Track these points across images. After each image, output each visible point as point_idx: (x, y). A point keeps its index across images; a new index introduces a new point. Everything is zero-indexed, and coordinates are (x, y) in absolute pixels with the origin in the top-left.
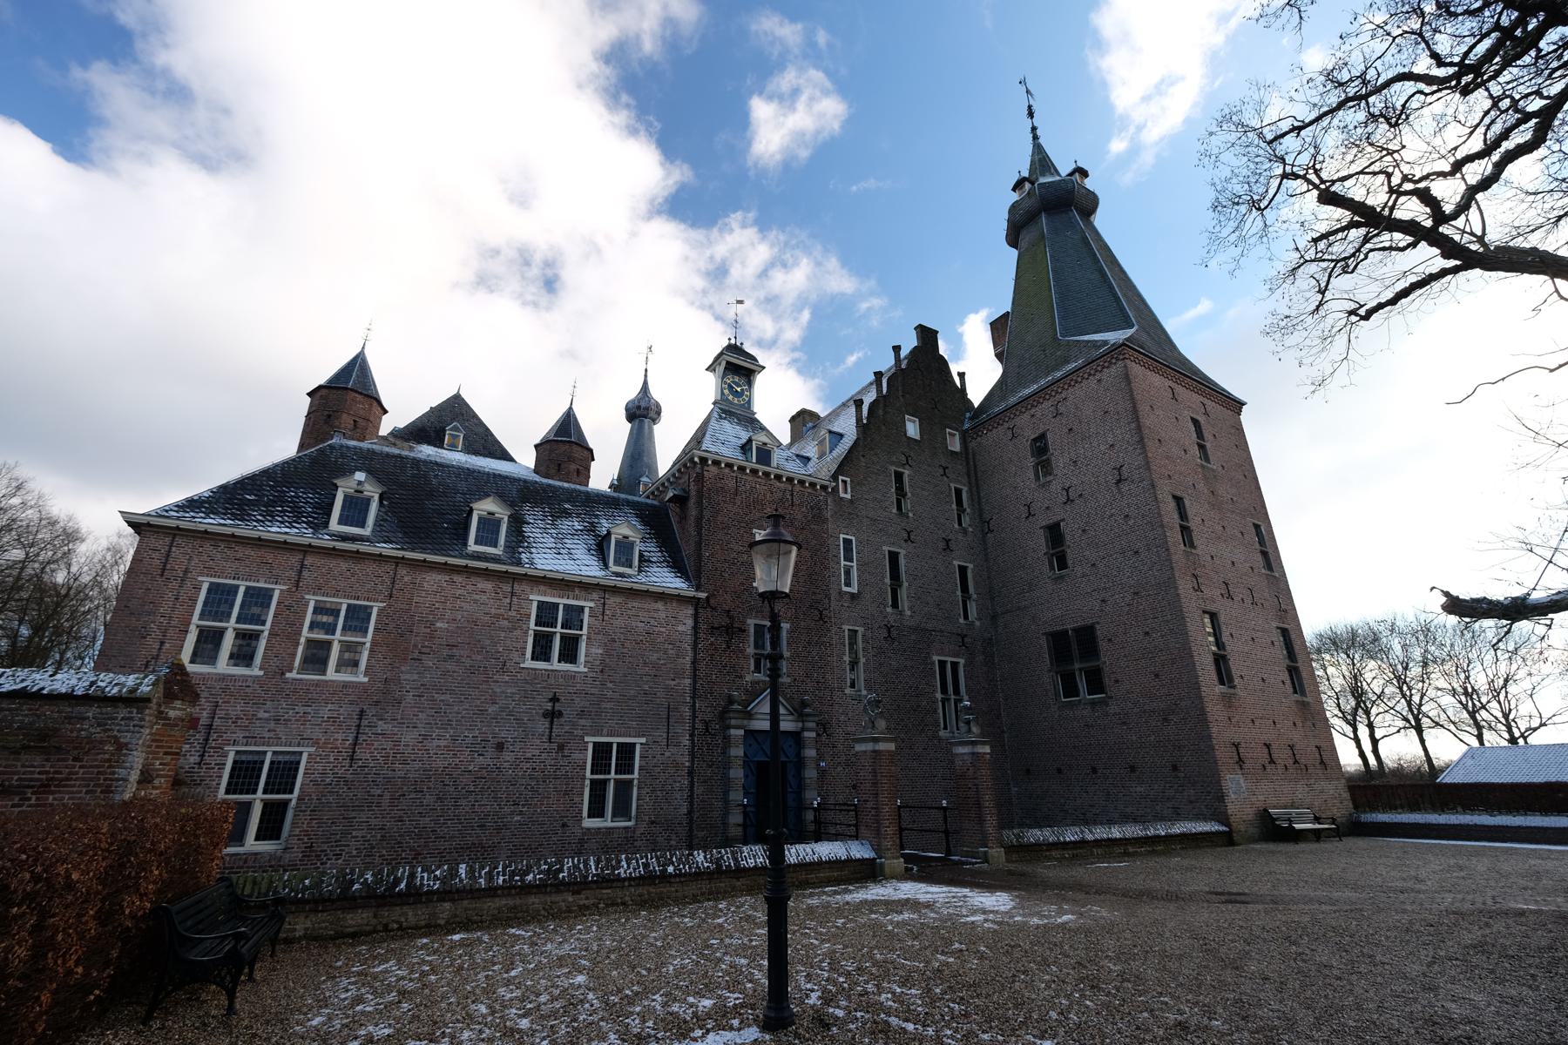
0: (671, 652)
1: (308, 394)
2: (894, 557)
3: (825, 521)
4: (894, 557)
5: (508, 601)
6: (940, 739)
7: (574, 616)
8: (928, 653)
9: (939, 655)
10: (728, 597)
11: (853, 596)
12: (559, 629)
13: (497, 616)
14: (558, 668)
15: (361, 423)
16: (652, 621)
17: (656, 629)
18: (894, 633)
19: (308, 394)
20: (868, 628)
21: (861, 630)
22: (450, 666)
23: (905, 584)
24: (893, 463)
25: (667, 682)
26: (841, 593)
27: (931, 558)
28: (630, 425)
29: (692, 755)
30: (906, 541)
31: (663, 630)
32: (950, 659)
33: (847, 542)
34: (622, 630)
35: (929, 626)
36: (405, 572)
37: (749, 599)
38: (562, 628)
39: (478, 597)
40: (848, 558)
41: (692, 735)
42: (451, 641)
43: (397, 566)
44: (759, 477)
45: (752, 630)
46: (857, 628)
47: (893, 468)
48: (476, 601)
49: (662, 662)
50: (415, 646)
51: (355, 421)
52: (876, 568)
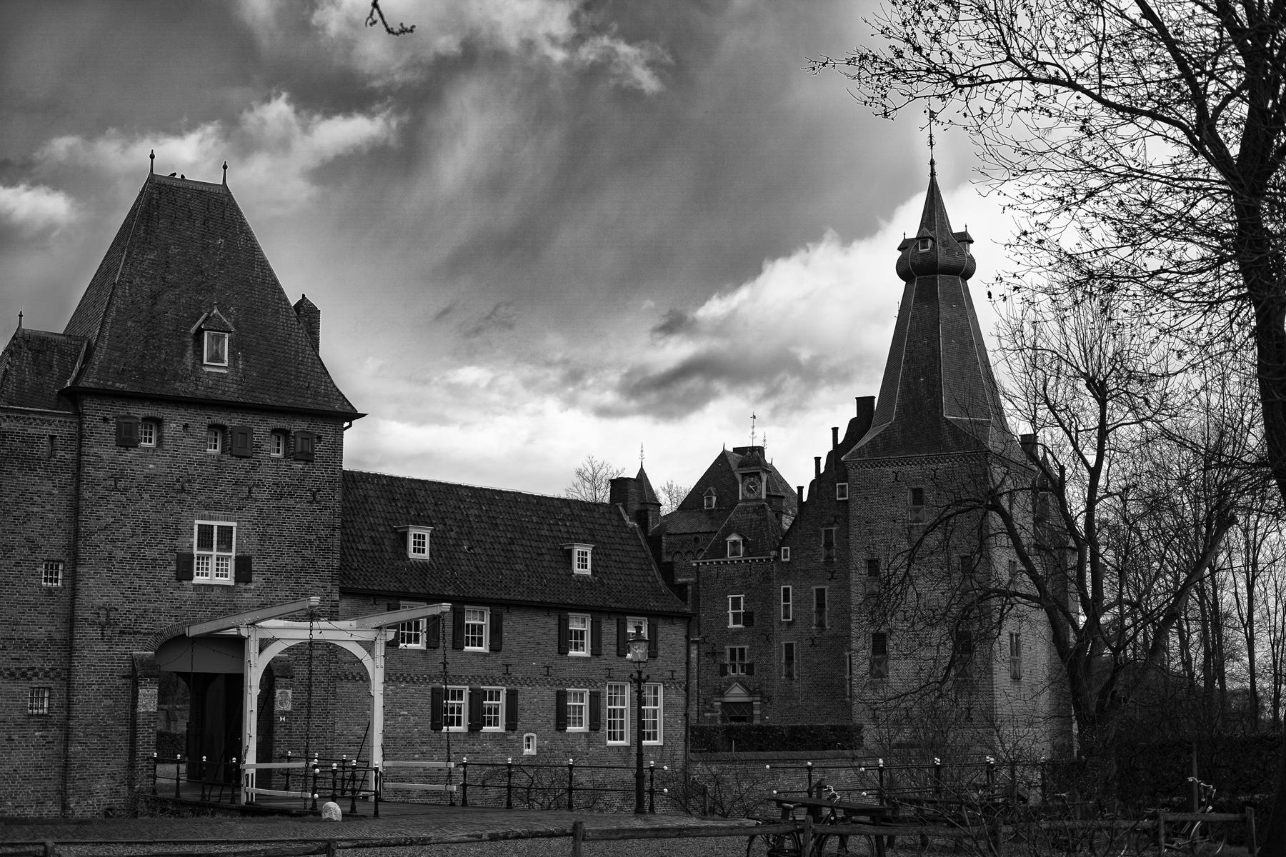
2: (821, 593)
4: (821, 593)
11: (789, 624)
18: (817, 641)
23: (827, 609)
24: (823, 526)
26: (781, 623)
29: (698, 714)
30: (830, 579)
33: (786, 590)
40: (787, 599)
41: (698, 705)
45: (728, 652)
47: (823, 530)
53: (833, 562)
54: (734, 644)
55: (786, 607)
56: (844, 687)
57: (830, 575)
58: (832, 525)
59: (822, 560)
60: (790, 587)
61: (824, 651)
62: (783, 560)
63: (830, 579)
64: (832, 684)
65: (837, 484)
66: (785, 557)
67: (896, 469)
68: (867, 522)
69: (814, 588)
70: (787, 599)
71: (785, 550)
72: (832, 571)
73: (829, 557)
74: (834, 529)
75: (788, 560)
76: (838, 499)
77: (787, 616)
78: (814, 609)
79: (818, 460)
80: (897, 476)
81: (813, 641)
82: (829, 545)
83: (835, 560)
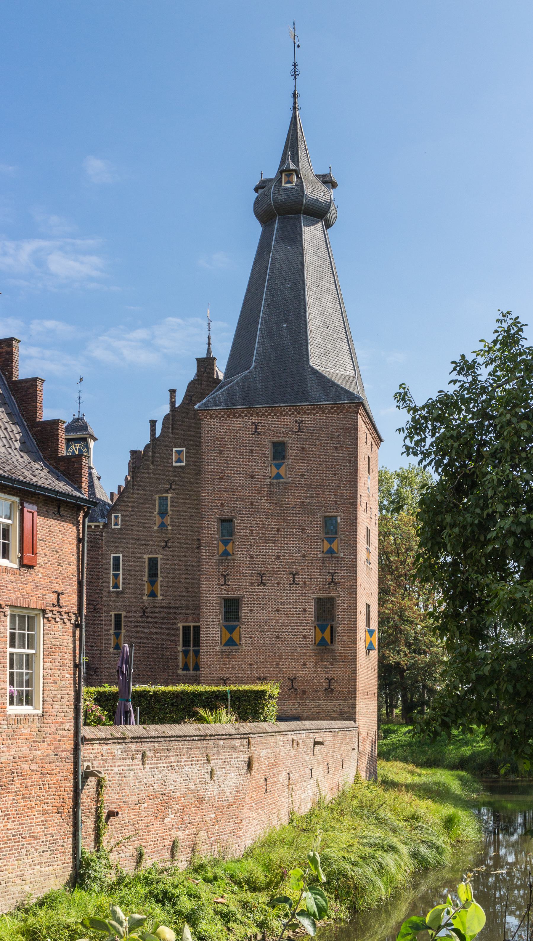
3: (100, 547)
6: (178, 675)
8: (175, 622)
9: (184, 622)
11: (118, 593)
18: (148, 612)
20: (128, 611)
21: (123, 613)
23: (160, 579)
24: (157, 492)
26: (110, 593)
27: (185, 556)
30: (163, 548)
32: (192, 625)
33: (117, 559)
35: (177, 604)
40: (116, 567)
46: (120, 612)
47: (157, 496)
52: (138, 571)
53: (167, 530)
55: (116, 576)
56: (176, 658)
57: (163, 544)
58: (167, 491)
59: (155, 528)
60: (121, 555)
61: (156, 622)
62: (113, 527)
63: (163, 548)
64: (163, 656)
65: (174, 449)
66: (116, 524)
67: (256, 420)
68: (222, 478)
69: (146, 557)
70: (116, 567)
71: (116, 517)
72: (166, 539)
73: (163, 526)
74: (170, 495)
75: (119, 527)
76: (174, 464)
77: (116, 586)
78: (146, 578)
79: (153, 423)
80: (256, 428)
81: (144, 611)
82: (163, 513)
83: (170, 528)
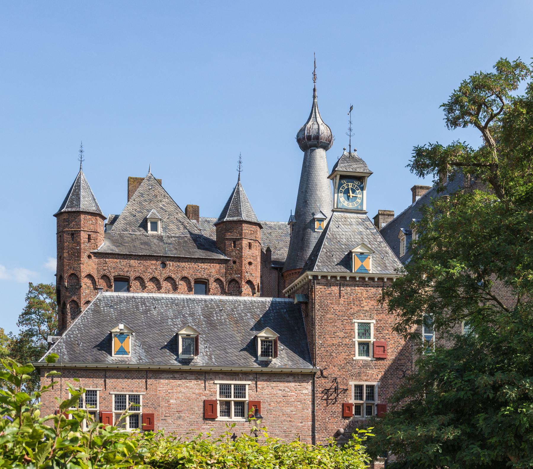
0: (299, 406)
1: (55, 216)
5: (203, 385)
7: (240, 390)
10: (336, 369)
12: (233, 398)
13: (200, 394)
14: (235, 420)
15: (93, 235)
16: (286, 389)
17: (289, 394)
19: (55, 216)
22: (180, 422)
25: (299, 424)
28: (304, 153)
31: (293, 394)
34: (268, 396)
36: (151, 375)
37: (350, 369)
38: (234, 397)
39: (188, 384)
42: (180, 409)
43: (147, 372)
44: (357, 281)
45: (353, 388)
48: (187, 387)
49: (294, 413)
50: (162, 413)
51: (89, 235)
54: (361, 380)
